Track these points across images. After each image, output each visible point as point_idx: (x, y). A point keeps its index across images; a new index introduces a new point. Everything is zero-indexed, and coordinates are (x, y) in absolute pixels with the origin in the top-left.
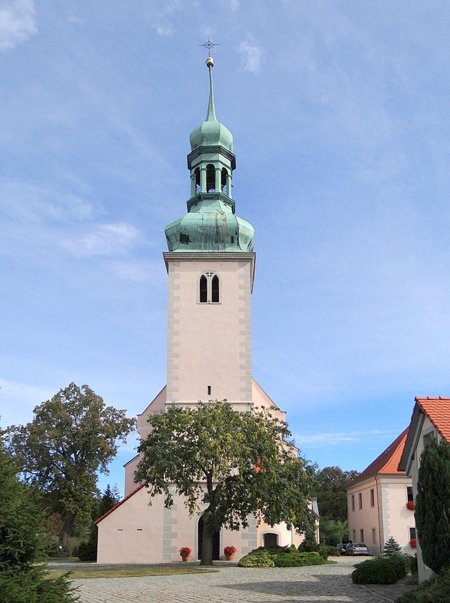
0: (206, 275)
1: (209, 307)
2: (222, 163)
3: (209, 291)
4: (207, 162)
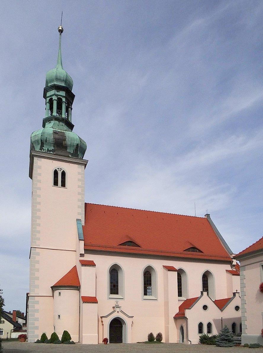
0: (58, 170)
1: (59, 189)
3: (60, 179)
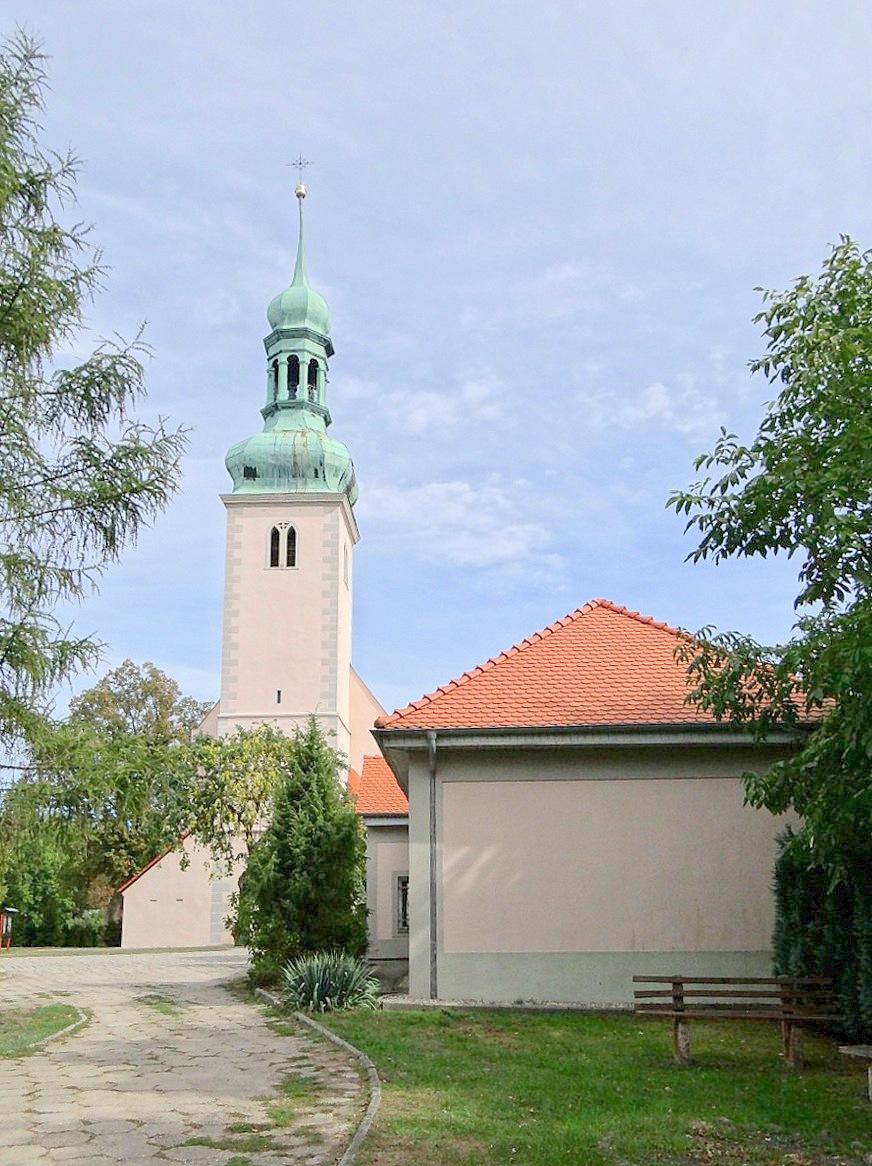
1: (283, 571)
2: (308, 352)
3: (283, 548)
4: (287, 351)
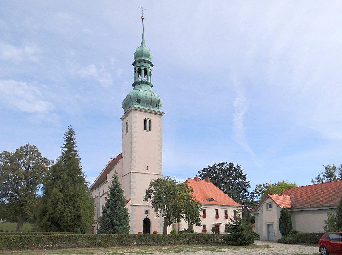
0: (147, 119)
1: (147, 132)
2: (150, 68)
3: (147, 125)
4: (145, 66)
